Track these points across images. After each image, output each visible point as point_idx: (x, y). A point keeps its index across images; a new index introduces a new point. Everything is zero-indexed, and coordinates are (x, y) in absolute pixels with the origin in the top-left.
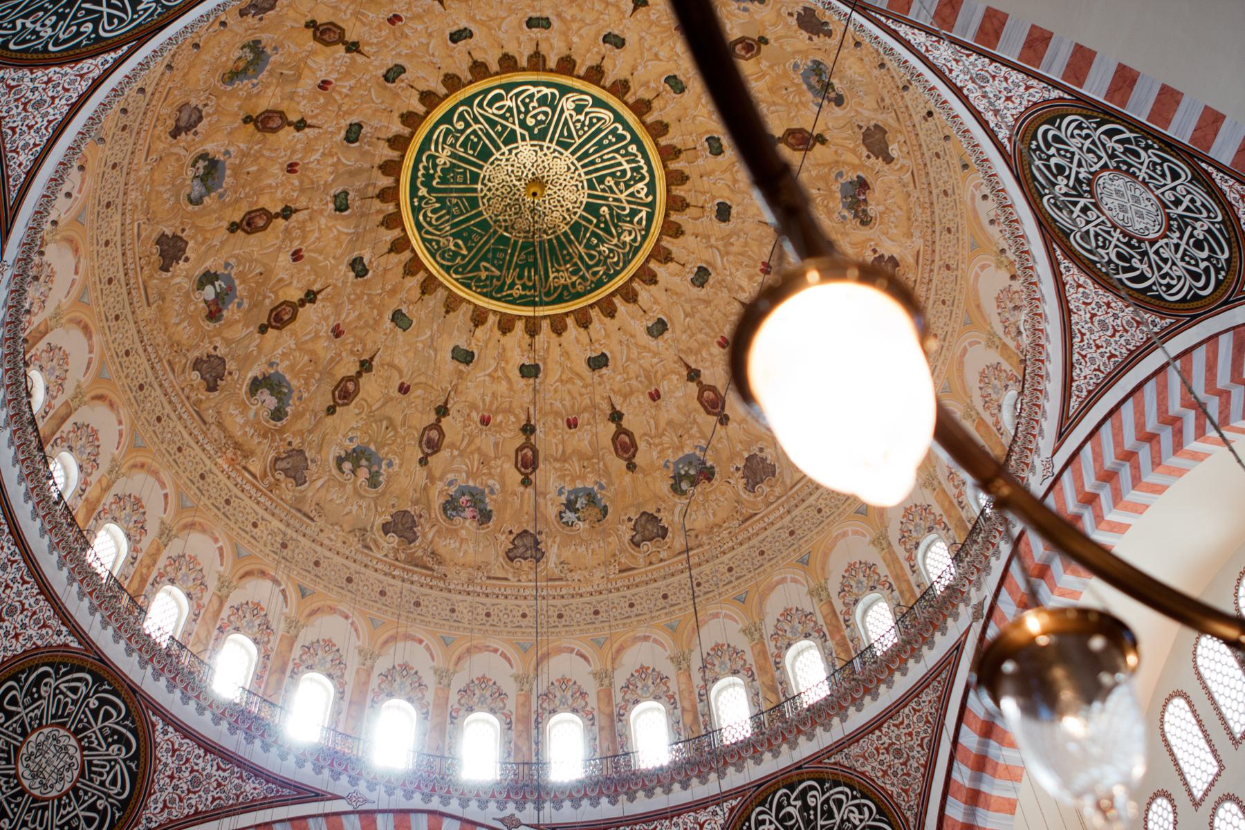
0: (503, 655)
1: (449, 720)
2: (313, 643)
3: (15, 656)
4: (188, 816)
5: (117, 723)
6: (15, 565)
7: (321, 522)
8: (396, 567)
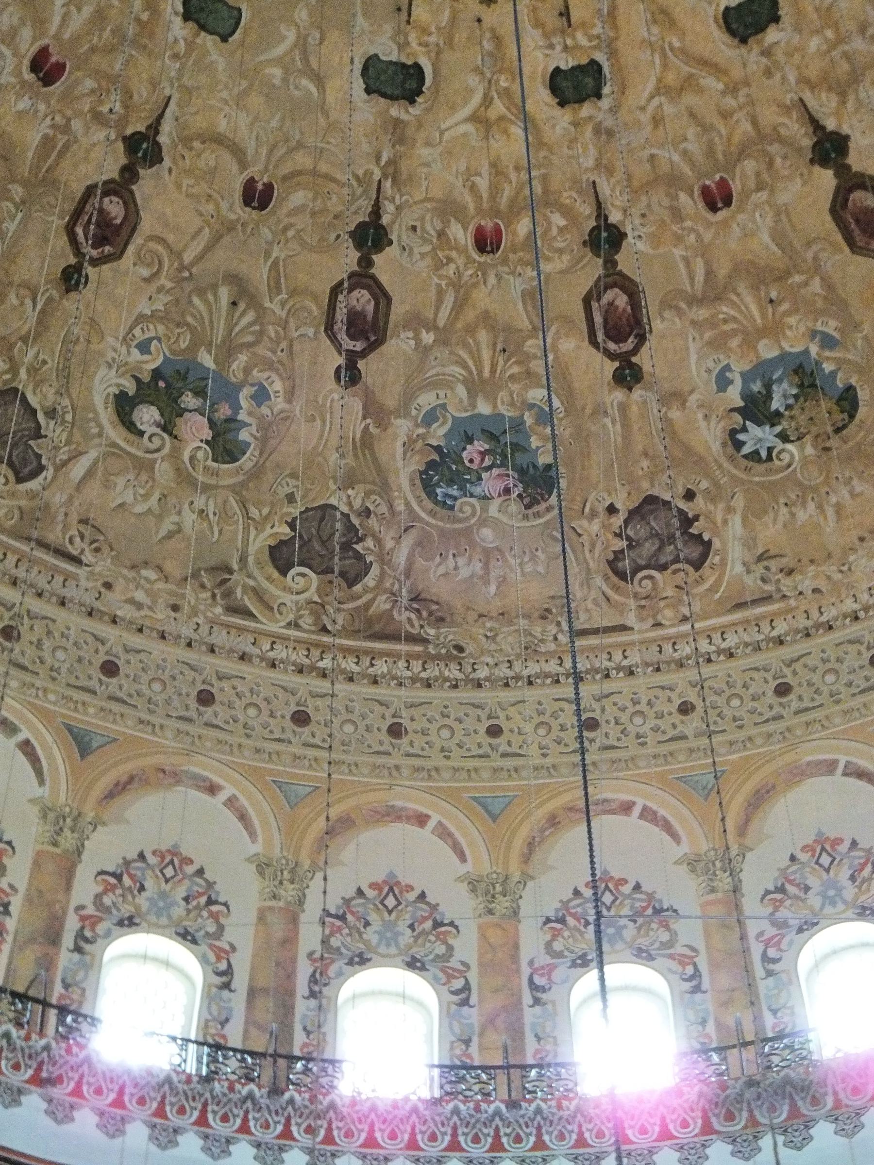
0: (648, 815)
1: (527, 998)
2: (127, 863)
7: (103, 565)
8: (324, 649)
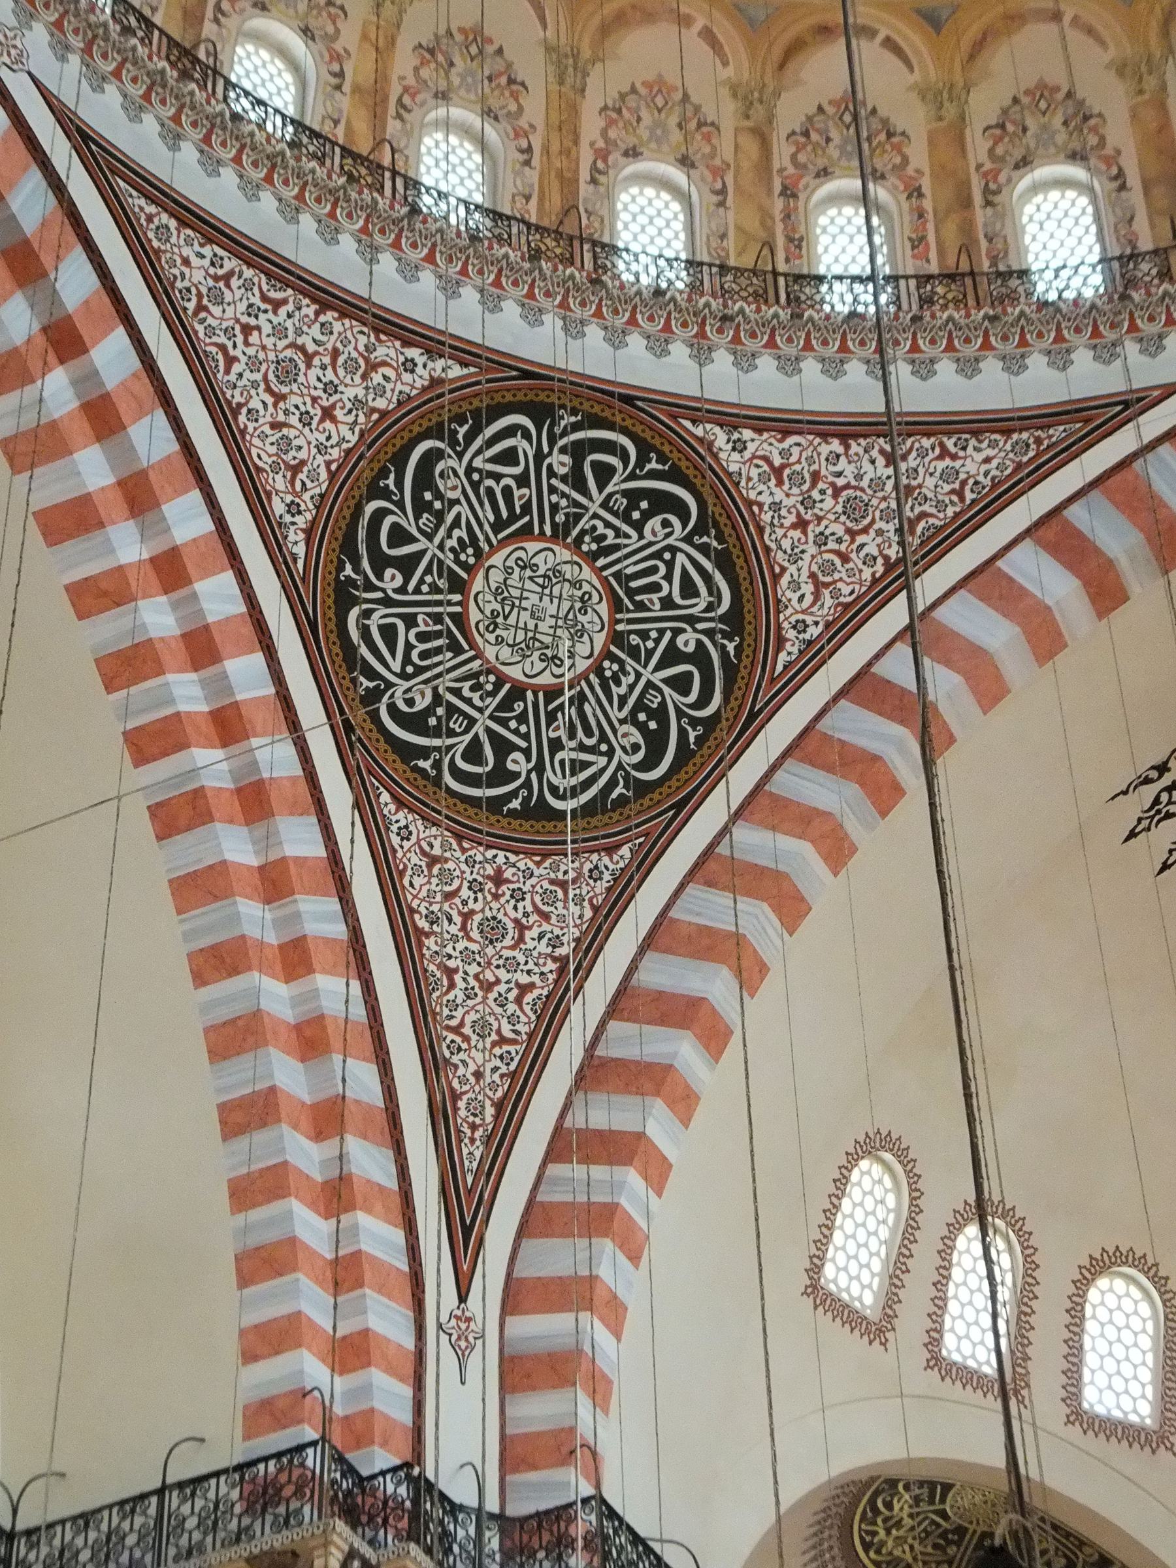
2: (1005, 111)
3: (348, 452)
4: (875, 581)
5: (632, 477)
6: (235, 282)
